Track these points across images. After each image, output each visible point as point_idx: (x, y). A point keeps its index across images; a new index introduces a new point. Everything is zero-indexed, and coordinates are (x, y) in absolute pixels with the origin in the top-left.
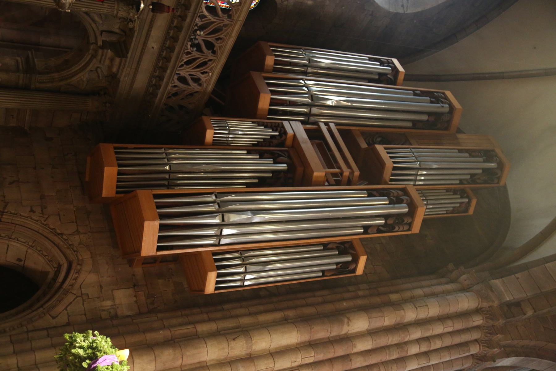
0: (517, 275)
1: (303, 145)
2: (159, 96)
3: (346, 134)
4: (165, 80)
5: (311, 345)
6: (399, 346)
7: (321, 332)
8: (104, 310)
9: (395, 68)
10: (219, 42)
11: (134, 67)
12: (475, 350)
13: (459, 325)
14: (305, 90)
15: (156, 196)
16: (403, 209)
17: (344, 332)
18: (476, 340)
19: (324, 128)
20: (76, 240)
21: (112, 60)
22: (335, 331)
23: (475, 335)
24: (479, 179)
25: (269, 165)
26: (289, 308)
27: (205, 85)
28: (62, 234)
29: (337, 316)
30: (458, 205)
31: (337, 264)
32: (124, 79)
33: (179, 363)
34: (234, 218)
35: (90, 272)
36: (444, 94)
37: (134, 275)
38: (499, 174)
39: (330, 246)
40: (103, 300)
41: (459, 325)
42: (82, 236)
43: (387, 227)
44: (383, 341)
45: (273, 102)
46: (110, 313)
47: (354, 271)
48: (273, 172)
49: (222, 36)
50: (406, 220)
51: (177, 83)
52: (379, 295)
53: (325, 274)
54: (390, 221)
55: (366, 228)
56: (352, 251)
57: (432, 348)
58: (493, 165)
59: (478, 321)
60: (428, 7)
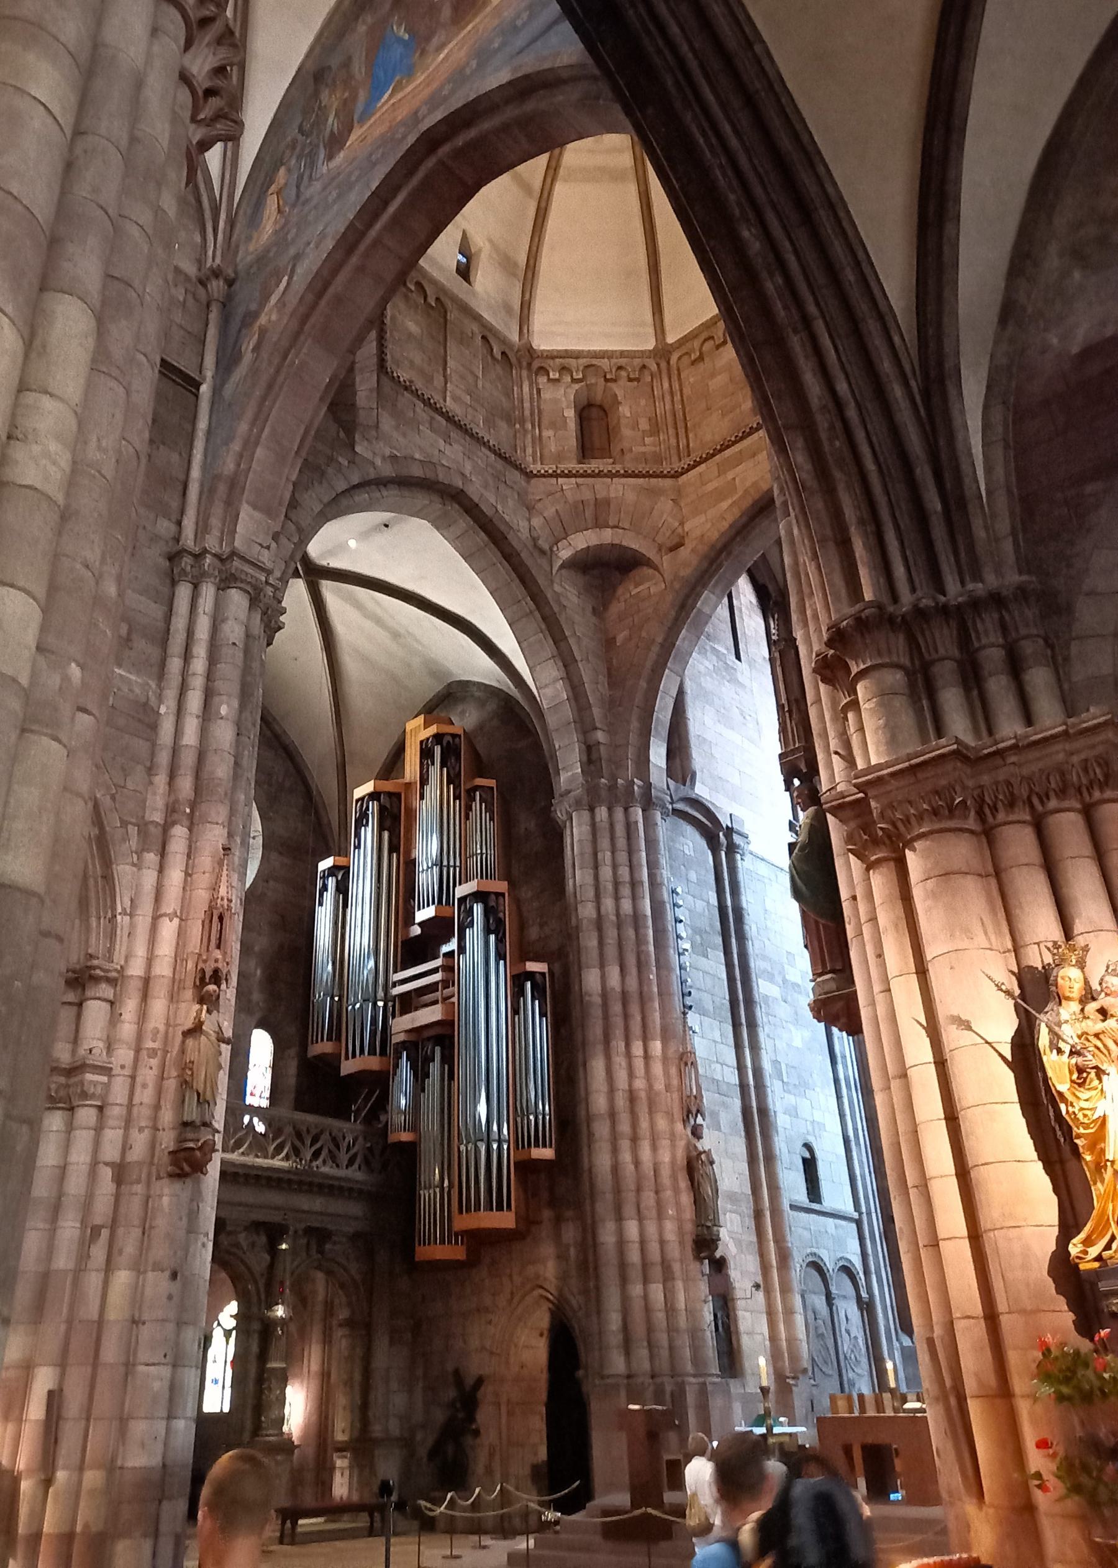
6: (619, 926)
7: (596, 1030)
12: (638, 814)
13: (604, 843)
15: (461, 1212)
16: (478, 909)
20: (517, 1280)
21: (335, 1243)
22: (597, 1012)
23: (619, 814)
24: (454, 768)
25: (435, 1068)
28: (512, 1293)
29: (584, 1007)
31: (533, 999)
32: (350, 1228)
36: (357, 801)
38: (450, 739)
41: (604, 843)
44: (611, 951)
45: (372, 1052)
47: (543, 974)
50: (492, 903)
51: (356, 1166)
58: (438, 750)
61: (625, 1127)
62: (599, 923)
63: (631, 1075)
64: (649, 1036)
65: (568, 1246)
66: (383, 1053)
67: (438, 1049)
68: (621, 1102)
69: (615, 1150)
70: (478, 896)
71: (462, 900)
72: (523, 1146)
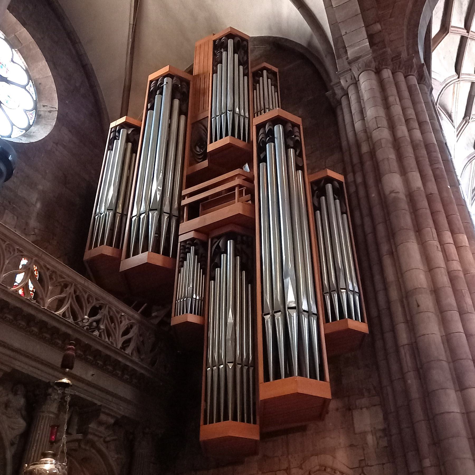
0: (343, 33)
1: (208, 223)
2: (142, 371)
3: (191, 180)
4: (128, 363)
5: (419, 230)
7: (405, 220)
8: (378, 443)
9: (122, 126)
10: (91, 301)
11: (110, 398)
14: (144, 216)
15: (267, 379)
16: (278, 130)
17: (405, 198)
18: (405, 77)
19: (185, 202)
21: (101, 423)
23: (401, 77)
26: (378, 250)
27: (132, 321)
29: (386, 204)
30: (269, 80)
31: (335, 199)
32: (123, 410)
33: (445, 364)
34: (291, 298)
35: (334, 458)
37: (337, 410)
39: (316, 204)
40: (367, 444)
42: (292, 466)
43: (297, 146)
46: (380, 437)
47: (340, 183)
48: (235, 256)
49: (86, 296)
50: (289, 128)
52: (362, 163)
53: (344, 211)
54: (291, 143)
55: (298, 167)
56: (323, 182)
57: (415, 118)
59: (387, 73)
60: (54, 86)
61: (450, 300)
62: (397, 144)
63: (447, 258)
64: (456, 230)
65: (364, 433)
66: (166, 253)
67: (230, 245)
68: (443, 279)
69: (444, 321)
70: (276, 120)
71: (259, 127)
72: (334, 318)
